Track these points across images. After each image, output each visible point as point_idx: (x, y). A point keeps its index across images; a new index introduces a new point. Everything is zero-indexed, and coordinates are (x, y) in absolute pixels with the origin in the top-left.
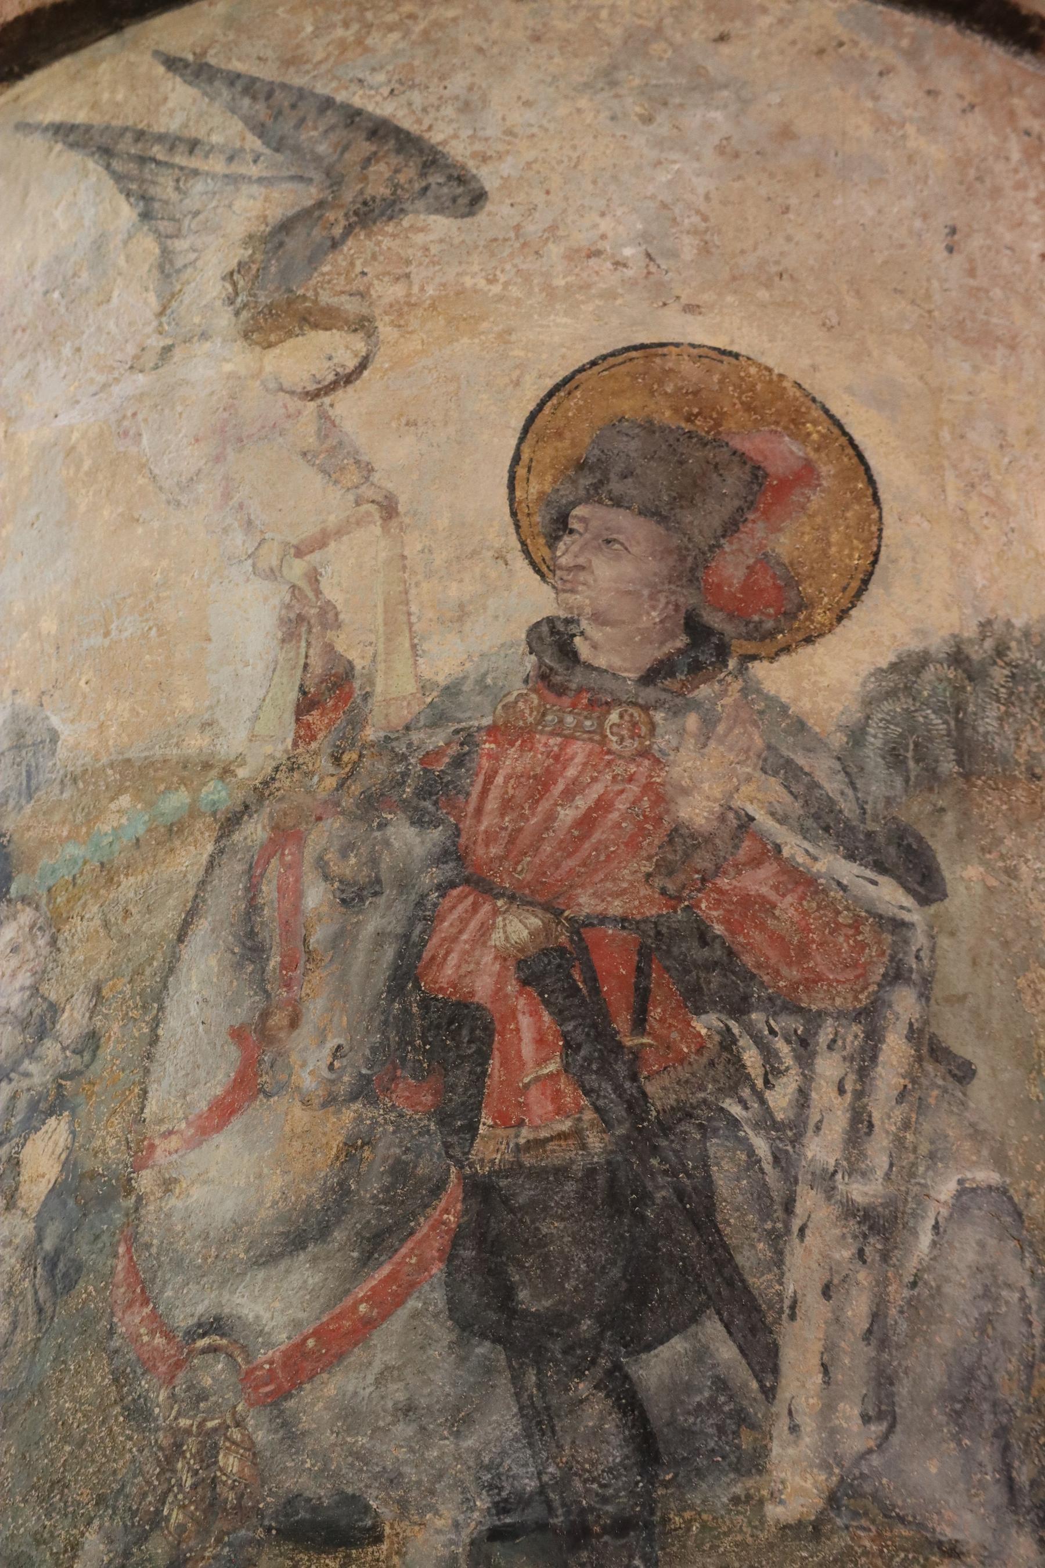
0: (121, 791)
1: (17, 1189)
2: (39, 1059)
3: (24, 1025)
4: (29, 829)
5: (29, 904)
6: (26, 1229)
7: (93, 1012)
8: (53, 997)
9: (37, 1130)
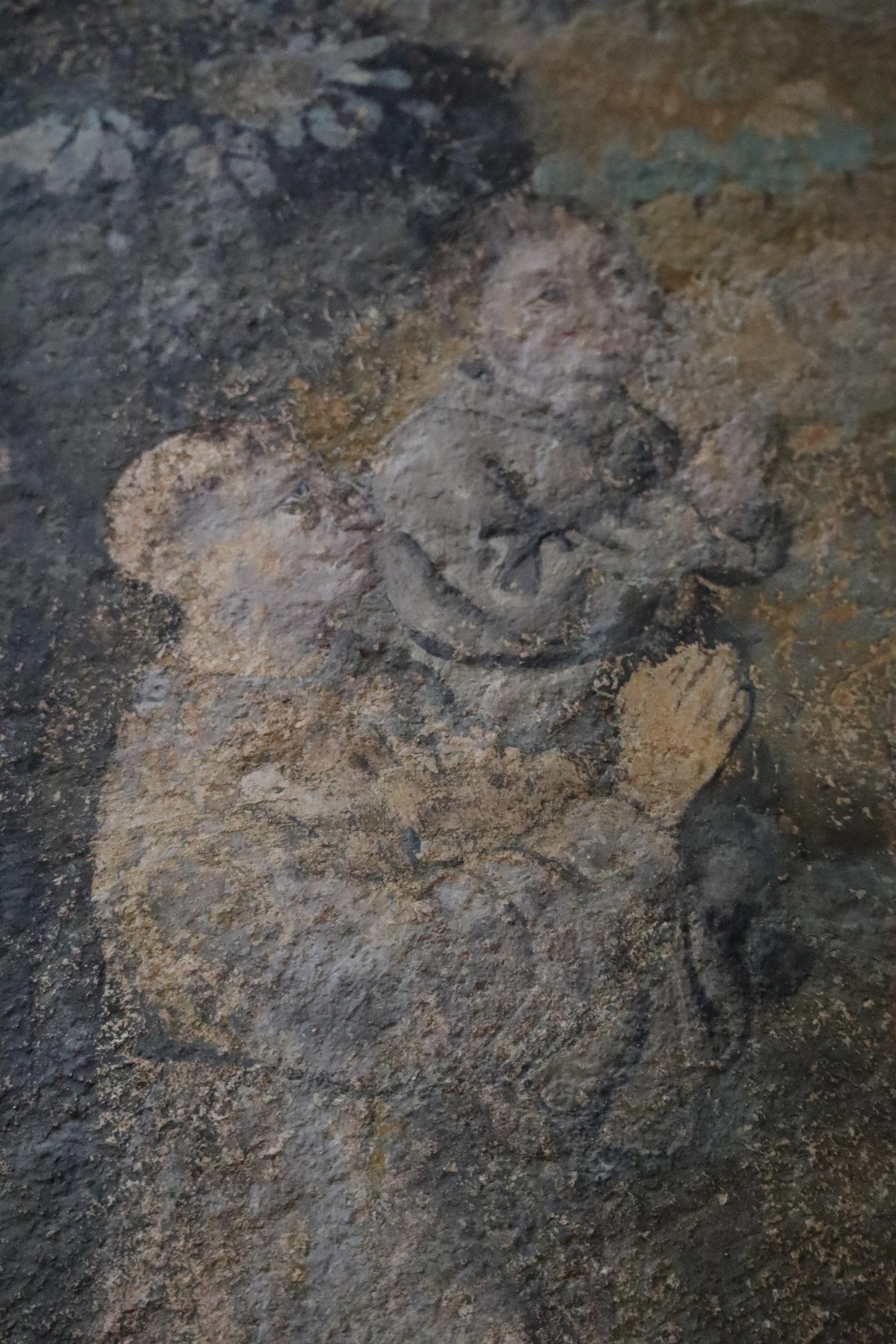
0: (794, 71)
1: (611, 761)
2: (642, 523)
3: (597, 443)
4: (571, 72)
5: (586, 218)
6: (651, 846)
7: (770, 474)
8: (667, 412)
9: (656, 660)
